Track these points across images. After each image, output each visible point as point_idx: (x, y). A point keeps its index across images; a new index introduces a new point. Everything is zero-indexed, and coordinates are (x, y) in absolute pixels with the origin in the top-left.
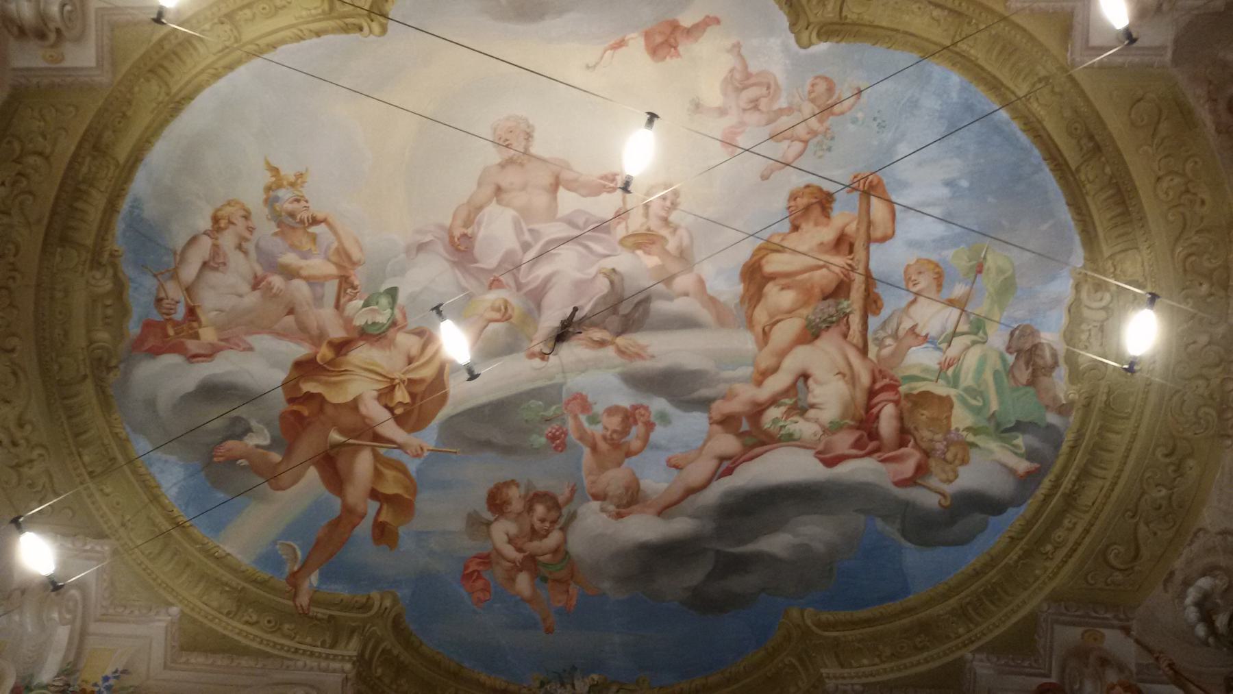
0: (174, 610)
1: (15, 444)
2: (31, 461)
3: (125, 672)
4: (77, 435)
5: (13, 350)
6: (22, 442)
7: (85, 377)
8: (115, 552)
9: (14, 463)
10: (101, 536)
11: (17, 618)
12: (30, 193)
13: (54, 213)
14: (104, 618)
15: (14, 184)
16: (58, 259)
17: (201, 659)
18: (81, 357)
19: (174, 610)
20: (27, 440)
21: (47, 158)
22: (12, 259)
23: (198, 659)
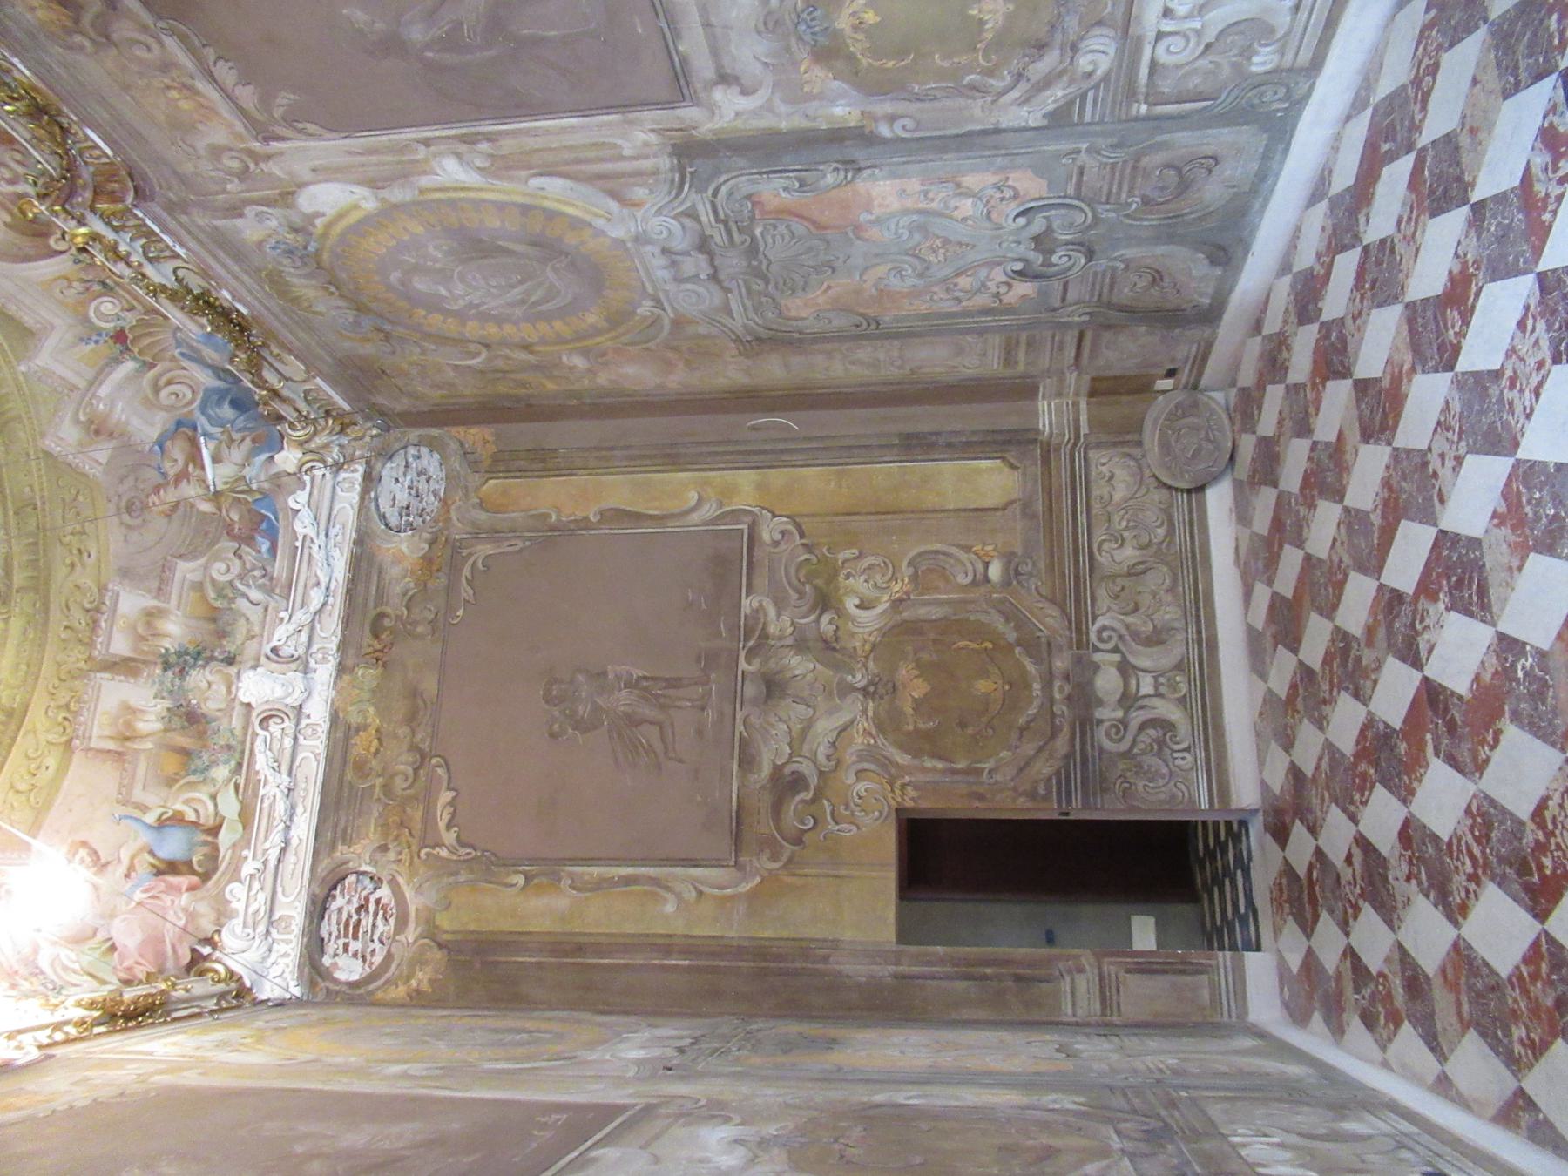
0: (23, 368)
1: (80, 551)
2: (72, 534)
3: (82, 340)
4: (36, 544)
5: (66, 627)
6: (75, 552)
7: (17, 591)
8: (43, 435)
9: (84, 537)
10: (48, 454)
11: (124, 417)
12: (29, 758)
13: (14, 739)
14: (73, 388)
15: (39, 767)
16: (18, 699)
17: (26, 318)
18: (17, 610)
19: (23, 368)
20: (71, 552)
21: (12, 787)
22: (52, 704)
23: (28, 320)
